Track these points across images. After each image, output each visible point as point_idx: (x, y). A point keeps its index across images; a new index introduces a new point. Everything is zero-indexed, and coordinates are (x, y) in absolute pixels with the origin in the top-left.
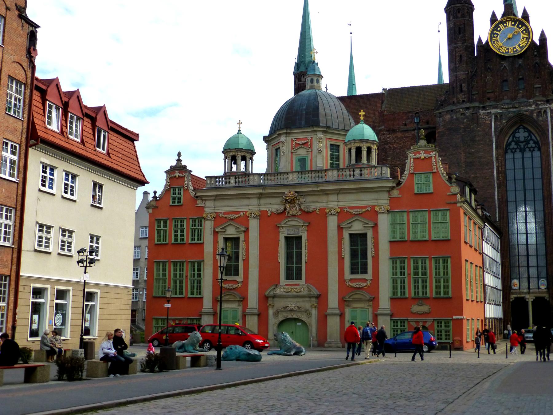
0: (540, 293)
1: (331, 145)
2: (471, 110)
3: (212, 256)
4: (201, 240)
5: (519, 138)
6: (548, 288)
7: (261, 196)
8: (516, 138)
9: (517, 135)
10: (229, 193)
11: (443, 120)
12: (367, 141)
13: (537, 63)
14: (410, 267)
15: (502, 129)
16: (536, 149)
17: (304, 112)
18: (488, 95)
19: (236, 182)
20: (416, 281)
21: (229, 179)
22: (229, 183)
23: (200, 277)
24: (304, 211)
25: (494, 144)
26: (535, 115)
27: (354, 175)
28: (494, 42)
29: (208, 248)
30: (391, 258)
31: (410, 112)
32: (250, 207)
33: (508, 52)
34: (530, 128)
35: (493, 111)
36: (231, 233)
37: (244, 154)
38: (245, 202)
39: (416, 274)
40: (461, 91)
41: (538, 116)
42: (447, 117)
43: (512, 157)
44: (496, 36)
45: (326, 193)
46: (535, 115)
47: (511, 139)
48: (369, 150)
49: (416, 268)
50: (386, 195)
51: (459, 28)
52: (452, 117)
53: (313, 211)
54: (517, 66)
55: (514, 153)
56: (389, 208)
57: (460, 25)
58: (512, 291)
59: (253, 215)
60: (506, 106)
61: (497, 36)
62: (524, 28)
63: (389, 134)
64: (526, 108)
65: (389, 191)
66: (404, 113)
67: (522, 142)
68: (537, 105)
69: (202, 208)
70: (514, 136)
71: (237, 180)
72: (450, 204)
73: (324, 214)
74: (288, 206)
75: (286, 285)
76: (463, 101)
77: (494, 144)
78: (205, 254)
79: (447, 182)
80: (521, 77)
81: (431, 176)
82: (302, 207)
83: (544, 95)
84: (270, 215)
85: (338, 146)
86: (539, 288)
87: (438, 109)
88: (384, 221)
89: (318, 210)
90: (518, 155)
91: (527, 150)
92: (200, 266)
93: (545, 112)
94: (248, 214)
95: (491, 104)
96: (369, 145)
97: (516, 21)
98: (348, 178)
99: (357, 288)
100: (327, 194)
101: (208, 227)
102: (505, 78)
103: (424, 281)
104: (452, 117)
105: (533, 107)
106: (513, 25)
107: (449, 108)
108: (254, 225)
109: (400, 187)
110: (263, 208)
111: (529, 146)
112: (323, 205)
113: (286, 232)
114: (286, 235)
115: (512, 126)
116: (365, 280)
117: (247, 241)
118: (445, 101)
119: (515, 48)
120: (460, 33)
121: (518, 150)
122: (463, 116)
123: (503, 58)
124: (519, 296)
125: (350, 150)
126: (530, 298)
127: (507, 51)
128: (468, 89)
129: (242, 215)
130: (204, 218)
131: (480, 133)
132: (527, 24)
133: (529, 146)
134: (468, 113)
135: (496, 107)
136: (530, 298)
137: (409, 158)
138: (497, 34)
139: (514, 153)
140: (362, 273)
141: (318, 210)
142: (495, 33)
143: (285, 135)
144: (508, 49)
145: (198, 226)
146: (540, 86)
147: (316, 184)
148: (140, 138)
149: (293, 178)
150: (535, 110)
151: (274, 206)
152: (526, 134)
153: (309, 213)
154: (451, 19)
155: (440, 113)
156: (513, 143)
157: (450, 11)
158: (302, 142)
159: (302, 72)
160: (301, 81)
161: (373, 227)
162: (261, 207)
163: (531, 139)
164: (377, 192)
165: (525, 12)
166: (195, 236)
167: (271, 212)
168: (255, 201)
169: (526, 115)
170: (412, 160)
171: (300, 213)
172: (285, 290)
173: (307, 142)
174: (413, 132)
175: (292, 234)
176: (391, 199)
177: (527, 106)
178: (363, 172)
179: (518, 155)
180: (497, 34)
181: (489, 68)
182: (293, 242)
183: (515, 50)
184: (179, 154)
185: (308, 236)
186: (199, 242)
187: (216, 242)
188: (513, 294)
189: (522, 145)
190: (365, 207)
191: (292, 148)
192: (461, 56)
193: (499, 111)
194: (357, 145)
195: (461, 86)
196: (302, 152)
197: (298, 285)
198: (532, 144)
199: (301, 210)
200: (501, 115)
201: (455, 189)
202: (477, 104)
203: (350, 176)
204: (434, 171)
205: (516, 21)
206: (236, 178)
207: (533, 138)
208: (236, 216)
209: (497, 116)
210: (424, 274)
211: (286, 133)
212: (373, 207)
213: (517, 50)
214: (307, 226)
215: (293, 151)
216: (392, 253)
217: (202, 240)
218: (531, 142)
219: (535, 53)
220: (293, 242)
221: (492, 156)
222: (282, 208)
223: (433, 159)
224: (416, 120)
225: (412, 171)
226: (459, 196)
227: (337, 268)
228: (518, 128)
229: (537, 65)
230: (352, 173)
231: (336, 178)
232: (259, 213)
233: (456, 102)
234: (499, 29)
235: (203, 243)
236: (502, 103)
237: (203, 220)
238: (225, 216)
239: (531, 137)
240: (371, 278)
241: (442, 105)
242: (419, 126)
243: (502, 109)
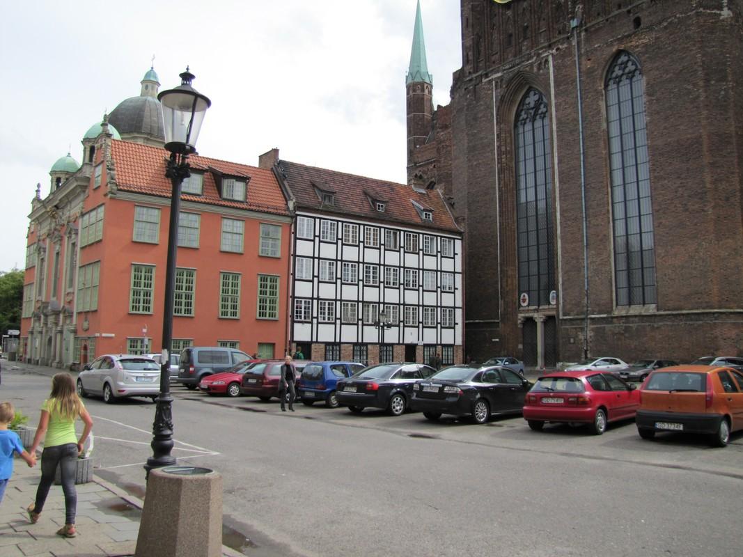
18: (493, 58)
41: (539, 69)
58: (521, 309)
63: (443, 131)
76: (470, 73)
86: (549, 304)
115: (516, 92)
124: (527, 315)
126: (539, 318)
131: (482, 108)
136: (539, 318)
184: (39, 186)
188: (521, 313)
192: (467, 19)
193: (499, 74)
195: (468, 55)
200: (501, 79)
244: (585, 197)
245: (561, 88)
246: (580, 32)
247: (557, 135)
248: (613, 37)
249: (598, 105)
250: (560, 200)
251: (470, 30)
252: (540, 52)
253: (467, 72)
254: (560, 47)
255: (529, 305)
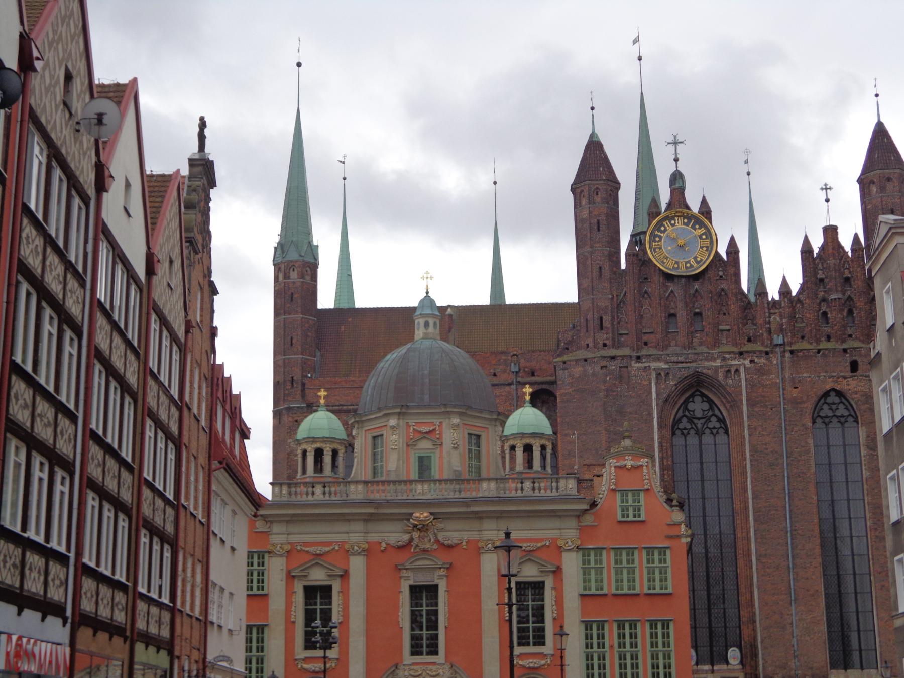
0: (729, 671)
1: (469, 434)
2: (617, 362)
3: (283, 617)
4: (263, 589)
5: (693, 411)
6: (742, 663)
7: (369, 519)
8: (689, 411)
9: (691, 406)
10: (317, 511)
11: (570, 375)
12: (540, 436)
13: (723, 290)
14: (611, 635)
15: (669, 396)
16: (721, 431)
17: (427, 380)
18: (645, 338)
19: (324, 493)
20: (622, 657)
21: (313, 487)
22: (313, 494)
23: (262, 651)
24: (443, 545)
25: (655, 420)
26: (721, 377)
27: (522, 489)
28: (655, 249)
29: (277, 603)
30: (583, 622)
31: (502, 352)
32: (351, 535)
33: (678, 268)
34: (711, 396)
35: (654, 365)
36: (318, 578)
37: (336, 446)
38: (343, 527)
39: (622, 645)
40: (601, 328)
41: (726, 377)
42: (577, 370)
43: (683, 443)
44: (657, 239)
45: (479, 517)
46: (721, 377)
47: (680, 413)
48: (543, 448)
49: (621, 636)
50: (573, 523)
51: (598, 222)
52: (585, 371)
53: (457, 545)
54: (692, 292)
55: (685, 436)
56: (579, 543)
57: (599, 215)
59: (356, 548)
60: (675, 359)
61: (660, 240)
62: (703, 230)
64: (707, 364)
65: (578, 517)
66: (492, 353)
67: (699, 419)
68: (724, 359)
69: (266, 534)
70: (686, 408)
71: (327, 489)
72: (670, 537)
73: (476, 550)
74: (416, 535)
75: (414, 664)
76: (605, 345)
77: (655, 420)
78: (270, 614)
79: (665, 504)
80: (697, 311)
81: (642, 495)
82: (440, 538)
83: (735, 344)
84: (386, 549)
85: (478, 437)
86: (728, 663)
87: (559, 356)
88: (571, 564)
89: (464, 543)
90: (693, 440)
91: (707, 431)
92: (263, 633)
93: (737, 371)
94: (347, 547)
95: (650, 353)
96: (543, 442)
97: (690, 218)
98: (513, 494)
99: (530, 668)
100: (481, 518)
101: (276, 568)
102: (672, 312)
103: (634, 657)
104: (585, 371)
105: (718, 363)
106: (685, 224)
107: (582, 354)
108: (357, 565)
109: (594, 510)
110: (374, 537)
111: (711, 425)
112: (474, 536)
113: (412, 578)
114: (412, 582)
115: (684, 391)
116: (543, 656)
117: (345, 592)
118: (571, 342)
119: (689, 262)
120: (599, 230)
121: (692, 432)
122: (604, 370)
123: (669, 277)
125: (513, 448)
127: (676, 266)
128: (613, 325)
129: (337, 548)
130: (269, 552)
132: (706, 222)
133: (711, 425)
134: (613, 366)
135: (658, 359)
137: (607, 466)
138: (660, 237)
139: (685, 436)
140: (535, 644)
141: (464, 543)
142: (657, 236)
143: (396, 417)
144: (677, 263)
145: (259, 565)
146: (728, 327)
147: (466, 503)
148: (252, 436)
149: (422, 491)
150: (721, 367)
151: (392, 534)
152: (706, 406)
153: (450, 547)
154: (583, 203)
155: (564, 362)
156: (685, 420)
157: (582, 191)
158: (427, 429)
159: (291, 261)
160: (289, 278)
161: (554, 572)
162: (369, 535)
163: (716, 416)
164: (560, 517)
165: (704, 202)
166: (252, 582)
167: (387, 544)
168: (359, 526)
169: (707, 375)
170: (613, 468)
171: (435, 547)
172: (412, 673)
173: (434, 430)
174: (507, 388)
175: (422, 579)
176: (581, 529)
177: (708, 360)
178: (537, 485)
179: (693, 440)
180: (660, 237)
181: (646, 292)
182: (424, 593)
183: (688, 265)
185: (448, 587)
186: (260, 592)
187: (290, 593)
189: (699, 424)
190: (541, 540)
191: (408, 436)
192: (600, 268)
193: (664, 366)
194: (527, 441)
195: (601, 319)
196: (425, 445)
197: (434, 664)
198: (714, 423)
199: (437, 541)
201: (678, 516)
202: (626, 351)
203: (516, 490)
204: (646, 487)
205: (690, 218)
206: (324, 487)
207: (717, 412)
208: (327, 549)
209: (660, 374)
210: (634, 645)
211: (399, 414)
212: (554, 541)
213: (691, 266)
214: (448, 568)
215: (410, 443)
216: (584, 611)
217: (265, 588)
218: (714, 419)
219: (721, 273)
220: (424, 593)
221: (653, 439)
222: (406, 537)
223: (645, 470)
224: (514, 368)
225: (613, 487)
226: (683, 526)
227: (497, 634)
228: (692, 396)
229: (723, 293)
230: (519, 485)
231: (493, 493)
232: (366, 546)
233: (591, 345)
234: (663, 228)
235: (266, 596)
236: (668, 352)
237: (266, 556)
238: (307, 549)
239: (713, 410)
240: (552, 652)
241: (567, 349)
242: (519, 379)
243: (667, 362)
244: (792, 544)
245: (757, 409)
246: (784, 351)
247: (752, 465)
248: (826, 372)
249: (806, 442)
250: (756, 542)
251: (607, 285)
252: (727, 356)
253: (601, 342)
254: (756, 360)
255: (697, 664)
